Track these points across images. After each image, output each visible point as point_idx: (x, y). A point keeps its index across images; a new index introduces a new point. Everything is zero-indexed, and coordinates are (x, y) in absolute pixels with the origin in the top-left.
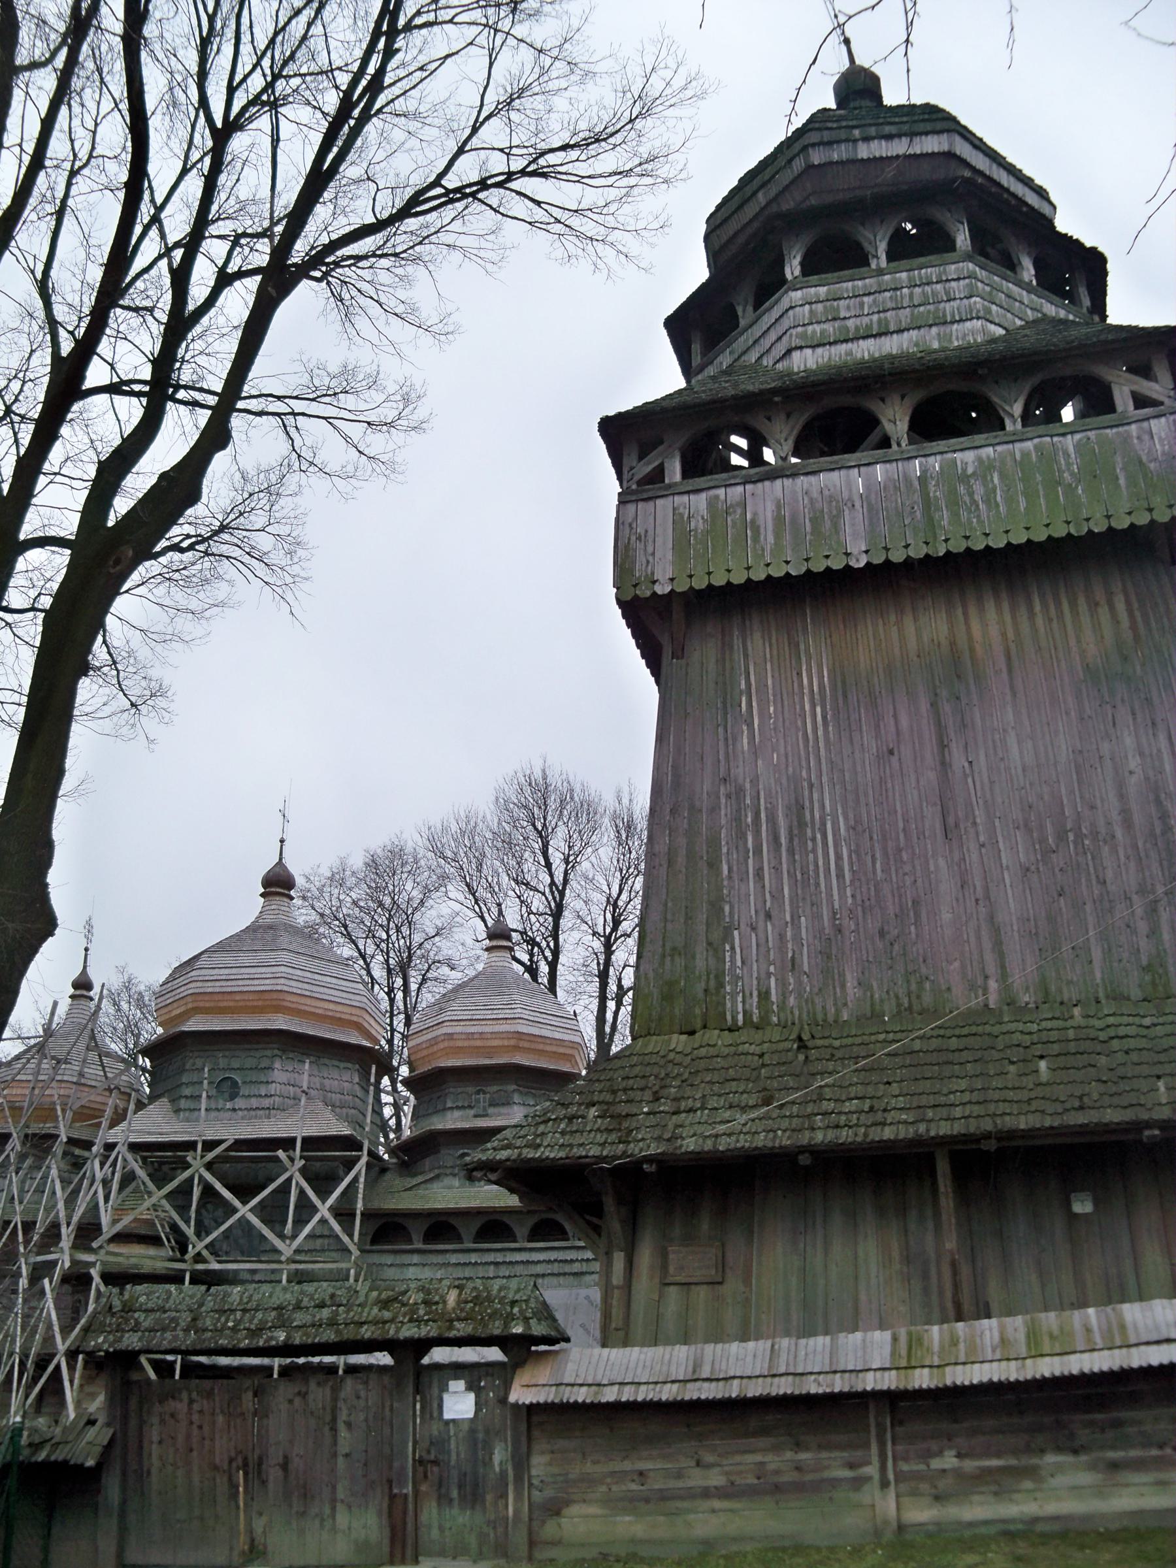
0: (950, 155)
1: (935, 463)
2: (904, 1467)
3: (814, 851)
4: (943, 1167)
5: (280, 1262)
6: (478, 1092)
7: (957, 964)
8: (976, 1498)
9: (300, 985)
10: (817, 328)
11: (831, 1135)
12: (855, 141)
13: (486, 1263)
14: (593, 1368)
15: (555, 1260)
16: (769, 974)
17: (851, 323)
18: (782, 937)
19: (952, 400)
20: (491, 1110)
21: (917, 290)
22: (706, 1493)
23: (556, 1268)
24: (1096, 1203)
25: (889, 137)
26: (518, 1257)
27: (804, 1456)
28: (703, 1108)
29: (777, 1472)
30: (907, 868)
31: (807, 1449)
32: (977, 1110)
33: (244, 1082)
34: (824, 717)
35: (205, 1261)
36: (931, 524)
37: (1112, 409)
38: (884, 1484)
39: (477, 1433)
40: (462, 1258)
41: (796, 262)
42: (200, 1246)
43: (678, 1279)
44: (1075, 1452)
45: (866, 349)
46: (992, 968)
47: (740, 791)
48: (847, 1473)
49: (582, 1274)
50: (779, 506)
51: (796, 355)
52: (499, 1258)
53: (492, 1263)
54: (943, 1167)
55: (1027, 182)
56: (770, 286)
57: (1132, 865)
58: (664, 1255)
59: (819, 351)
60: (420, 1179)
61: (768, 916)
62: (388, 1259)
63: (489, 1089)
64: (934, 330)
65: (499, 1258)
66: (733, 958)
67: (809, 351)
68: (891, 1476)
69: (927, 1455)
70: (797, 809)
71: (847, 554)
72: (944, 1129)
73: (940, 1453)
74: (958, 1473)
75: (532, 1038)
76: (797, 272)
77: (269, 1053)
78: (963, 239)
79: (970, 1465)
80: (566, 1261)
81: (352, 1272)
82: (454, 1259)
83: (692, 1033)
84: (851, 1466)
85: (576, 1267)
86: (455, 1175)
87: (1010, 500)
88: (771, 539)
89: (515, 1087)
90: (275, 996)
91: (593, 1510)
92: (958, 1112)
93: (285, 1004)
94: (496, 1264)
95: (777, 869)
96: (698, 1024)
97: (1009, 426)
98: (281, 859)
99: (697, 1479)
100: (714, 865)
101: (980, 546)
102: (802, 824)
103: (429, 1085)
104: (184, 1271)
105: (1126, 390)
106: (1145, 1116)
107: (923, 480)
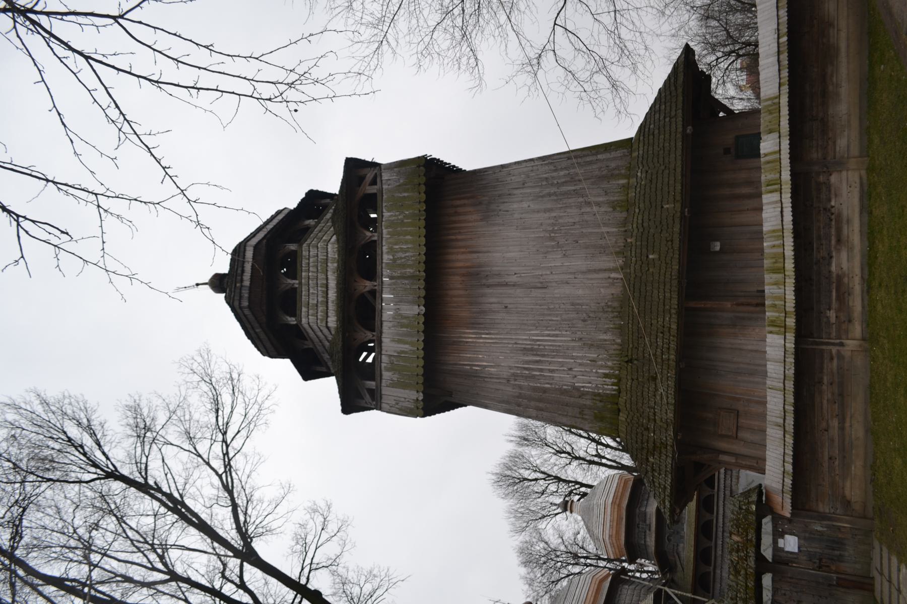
0: (256, 247)
1: (386, 272)
2: (834, 334)
3: (544, 346)
4: (692, 304)
7: (602, 290)
8: (851, 304)
10: (319, 314)
11: (672, 352)
12: (242, 286)
14: (775, 472)
16: (596, 372)
17: (320, 299)
18: (580, 364)
19: (360, 261)
20: (648, 522)
21: (311, 269)
22: (842, 429)
24: (717, 240)
25: (243, 271)
26: (721, 520)
27: (825, 380)
28: (654, 408)
29: (833, 394)
30: (557, 306)
31: (822, 378)
32: (668, 286)
34: (487, 334)
36: (412, 277)
37: (375, 195)
38: (842, 344)
39: (805, 537)
41: (289, 319)
43: (734, 431)
44: (831, 257)
45: (332, 295)
46: (606, 275)
47: (514, 375)
48: (835, 361)
50: (393, 341)
51: (330, 325)
52: (720, 529)
54: (692, 304)
55: (273, 217)
56: (298, 332)
57: (568, 210)
58: (723, 436)
59: (329, 314)
60: (678, 563)
61: (570, 369)
64: (329, 264)
65: (720, 529)
66: (588, 387)
67: (329, 319)
68: (838, 341)
69: (828, 323)
70: (525, 351)
71: (419, 314)
72: (675, 301)
73: (828, 318)
74: (838, 311)
76: (294, 319)
78: (293, 247)
79: (834, 304)
82: (719, 552)
83: (619, 410)
84: (832, 359)
87: (406, 242)
88: (407, 346)
91: (848, 484)
92: (668, 295)
94: (723, 531)
95: (550, 363)
96: (616, 406)
97: (375, 238)
99: (835, 432)
100: (545, 391)
101: (424, 258)
102: (532, 350)
103: (633, 551)
105: (368, 188)
106: (679, 214)
107: (391, 278)
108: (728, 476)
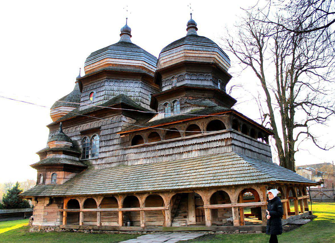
6: (173, 78)
13: (169, 148)
15: (196, 144)
26: (181, 144)
40: (160, 147)
49: (207, 148)
52: (173, 145)
53: (171, 147)
65: (173, 145)
77: (104, 81)
80: (200, 144)
82: (157, 147)
85: (205, 146)
94: (173, 148)
98: (126, 24)
108: (219, 144)
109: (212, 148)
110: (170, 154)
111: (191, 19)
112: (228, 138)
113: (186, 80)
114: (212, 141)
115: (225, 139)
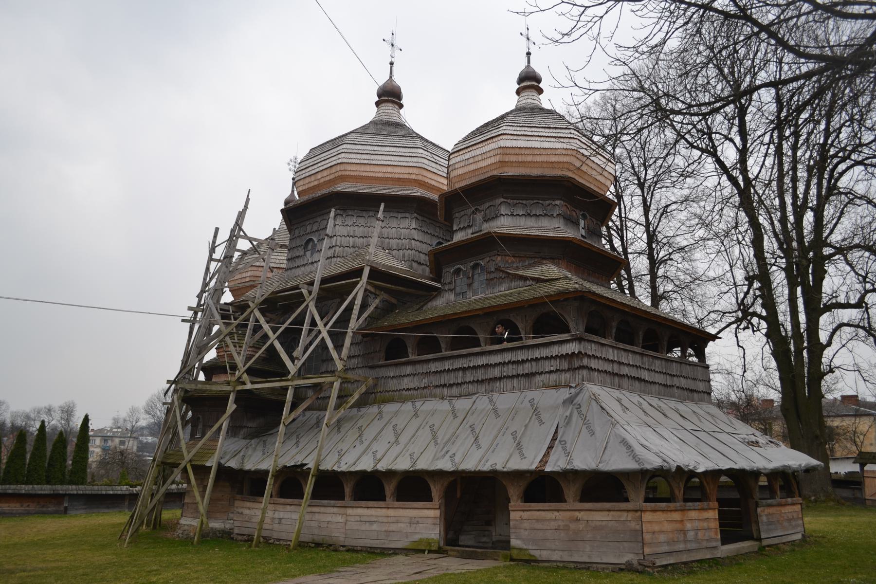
5: (288, 380)
6: (474, 213)
9: (359, 156)
15: (509, 362)
23: (510, 370)
33: (319, 240)
35: (244, 383)
42: (243, 369)
49: (532, 374)
53: (460, 368)
62: (391, 372)
63: (483, 207)
65: (465, 362)
75: (517, 151)
81: (337, 385)
82: (434, 367)
85: (527, 368)
86: (451, 290)
89: (503, 200)
90: (338, 168)
93: (347, 173)
94: (464, 369)
98: (391, 77)
104: (230, 392)
108: (555, 365)
109: (542, 373)
110: (458, 384)
111: (528, 66)
112: (573, 353)
113: (502, 218)
114: (542, 358)
115: (567, 354)
